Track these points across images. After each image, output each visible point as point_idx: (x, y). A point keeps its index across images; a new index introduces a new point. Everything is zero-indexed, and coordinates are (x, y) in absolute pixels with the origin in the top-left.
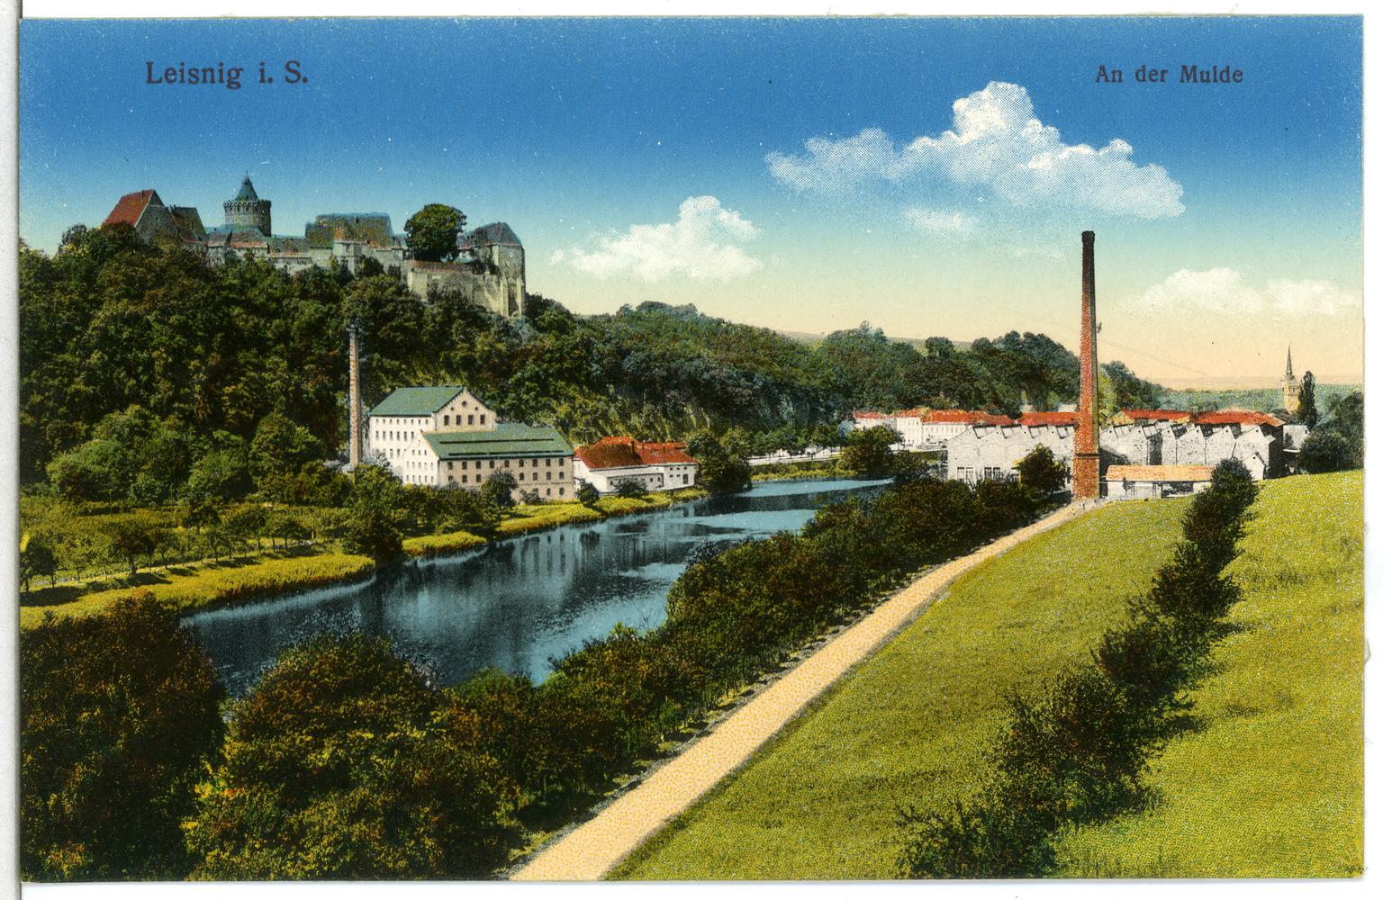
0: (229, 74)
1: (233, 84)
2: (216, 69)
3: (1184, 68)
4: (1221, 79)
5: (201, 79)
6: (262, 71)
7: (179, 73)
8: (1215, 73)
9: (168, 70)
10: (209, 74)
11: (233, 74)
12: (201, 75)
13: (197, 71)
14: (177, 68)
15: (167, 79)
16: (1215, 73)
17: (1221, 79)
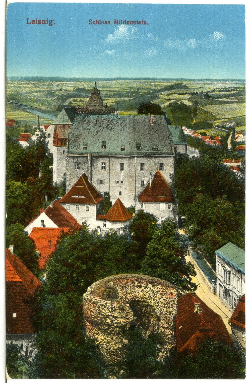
0: (49, 21)
1: (50, 24)
3: (115, 20)
5: (42, 23)
7: (36, 21)
10: (44, 21)
11: (51, 22)
12: (42, 21)
13: (41, 20)
14: (35, 20)
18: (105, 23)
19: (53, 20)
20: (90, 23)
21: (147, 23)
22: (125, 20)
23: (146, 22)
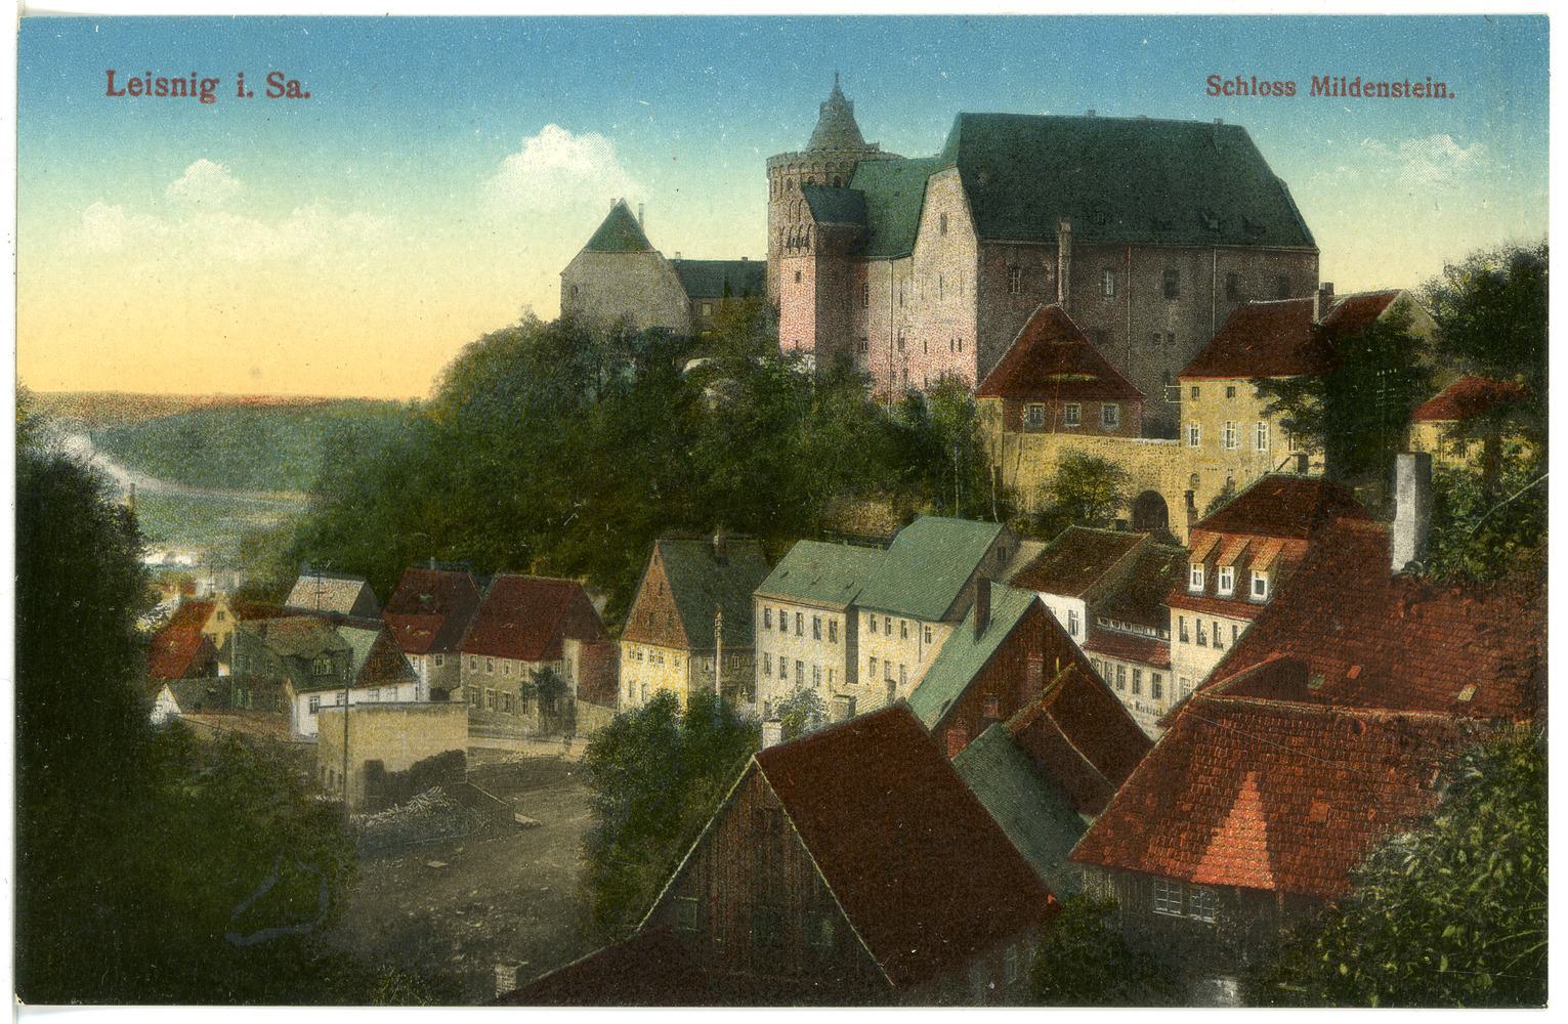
0: (203, 85)
1: (206, 96)
2: (188, 78)
3: (1315, 79)
4: (1351, 90)
5: (171, 91)
6: (240, 83)
7: (145, 86)
8: (1344, 85)
9: (131, 81)
11: (208, 85)
12: (170, 87)
13: (165, 80)
15: (130, 91)
16: (1344, 85)
17: (1351, 90)
18: (1272, 89)
19: (217, 81)
20: (1214, 90)
21: (1448, 93)
22: (1358, 78)
23: (1443, 85)
